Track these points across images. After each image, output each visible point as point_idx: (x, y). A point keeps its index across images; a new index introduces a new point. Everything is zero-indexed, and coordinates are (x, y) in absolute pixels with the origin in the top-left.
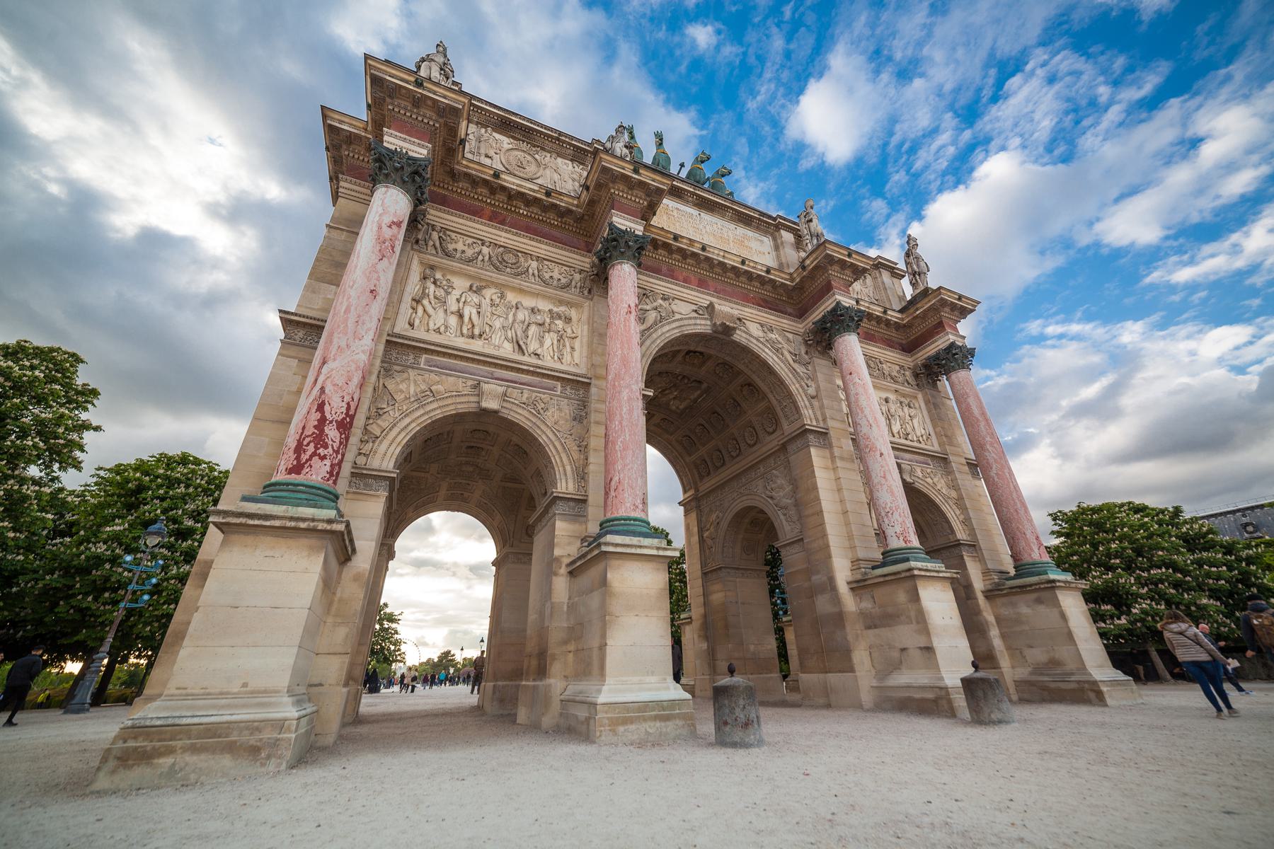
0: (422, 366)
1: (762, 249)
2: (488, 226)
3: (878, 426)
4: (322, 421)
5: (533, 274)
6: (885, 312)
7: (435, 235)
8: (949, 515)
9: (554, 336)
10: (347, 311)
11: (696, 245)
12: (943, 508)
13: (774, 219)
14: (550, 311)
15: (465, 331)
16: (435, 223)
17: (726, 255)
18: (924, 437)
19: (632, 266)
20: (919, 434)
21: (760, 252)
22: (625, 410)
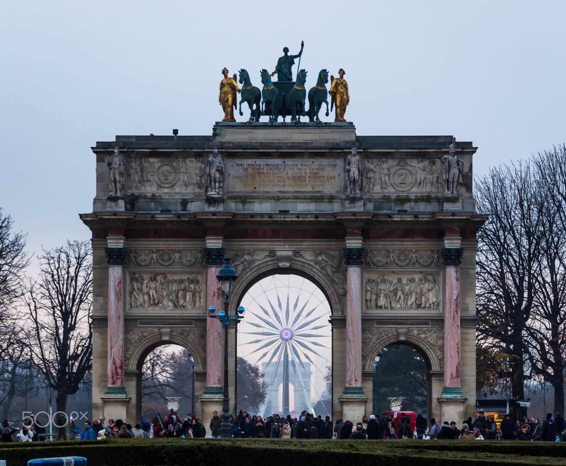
0: (139, 326)
1: (333, 174)
2: (154, 241)
3: (352, 326)
4: (116, 368)
5: (177, 262)
6: (416, 216)
7: (132, 255)
8: (430, 357)
9: (191, 294)
10: (114, 328)
11: (265, 216)
12: (428, 352)
13: (342, 149)
14: (188, 279)
15: (152, 303)
16: (131, 249)
17: (285, 216)
18: (436, 303)
19: (216, 267)
20: (431, 302)
21: (331, 178)
22: (211, 345)
